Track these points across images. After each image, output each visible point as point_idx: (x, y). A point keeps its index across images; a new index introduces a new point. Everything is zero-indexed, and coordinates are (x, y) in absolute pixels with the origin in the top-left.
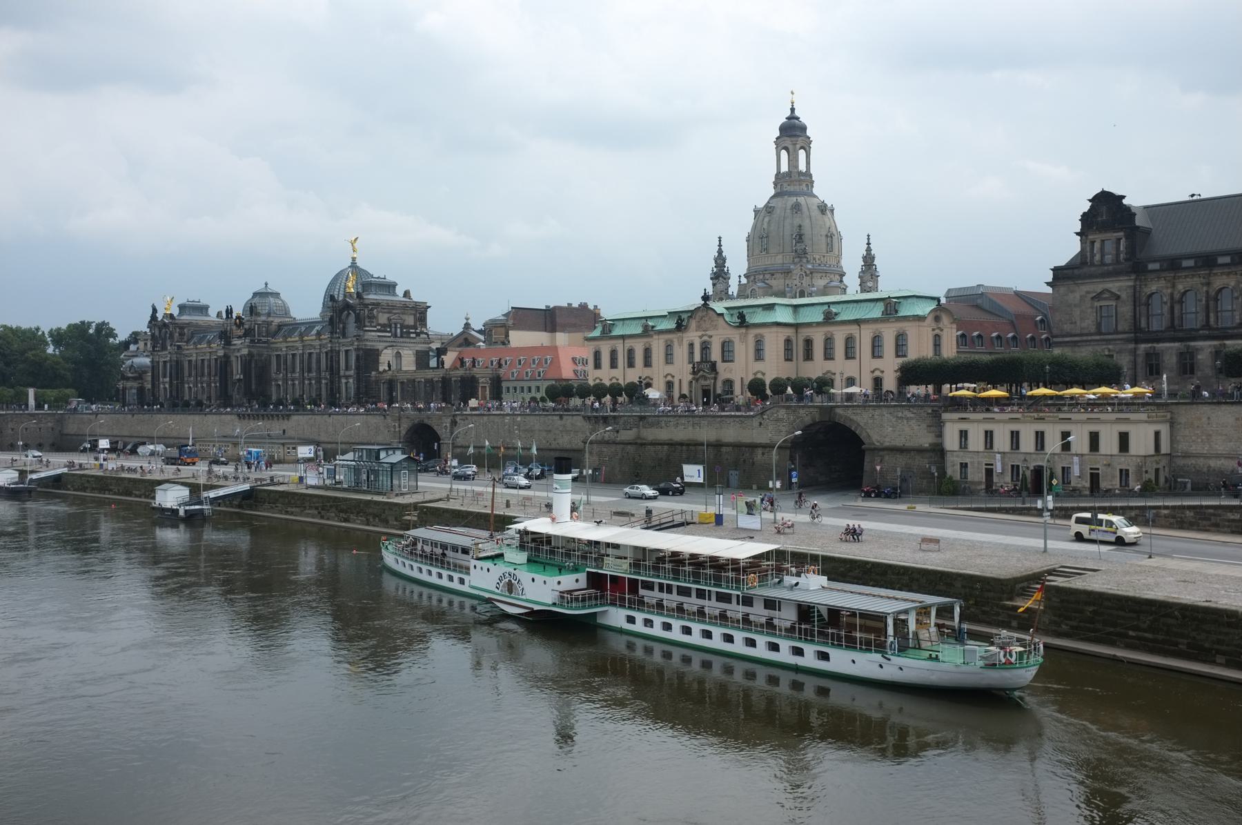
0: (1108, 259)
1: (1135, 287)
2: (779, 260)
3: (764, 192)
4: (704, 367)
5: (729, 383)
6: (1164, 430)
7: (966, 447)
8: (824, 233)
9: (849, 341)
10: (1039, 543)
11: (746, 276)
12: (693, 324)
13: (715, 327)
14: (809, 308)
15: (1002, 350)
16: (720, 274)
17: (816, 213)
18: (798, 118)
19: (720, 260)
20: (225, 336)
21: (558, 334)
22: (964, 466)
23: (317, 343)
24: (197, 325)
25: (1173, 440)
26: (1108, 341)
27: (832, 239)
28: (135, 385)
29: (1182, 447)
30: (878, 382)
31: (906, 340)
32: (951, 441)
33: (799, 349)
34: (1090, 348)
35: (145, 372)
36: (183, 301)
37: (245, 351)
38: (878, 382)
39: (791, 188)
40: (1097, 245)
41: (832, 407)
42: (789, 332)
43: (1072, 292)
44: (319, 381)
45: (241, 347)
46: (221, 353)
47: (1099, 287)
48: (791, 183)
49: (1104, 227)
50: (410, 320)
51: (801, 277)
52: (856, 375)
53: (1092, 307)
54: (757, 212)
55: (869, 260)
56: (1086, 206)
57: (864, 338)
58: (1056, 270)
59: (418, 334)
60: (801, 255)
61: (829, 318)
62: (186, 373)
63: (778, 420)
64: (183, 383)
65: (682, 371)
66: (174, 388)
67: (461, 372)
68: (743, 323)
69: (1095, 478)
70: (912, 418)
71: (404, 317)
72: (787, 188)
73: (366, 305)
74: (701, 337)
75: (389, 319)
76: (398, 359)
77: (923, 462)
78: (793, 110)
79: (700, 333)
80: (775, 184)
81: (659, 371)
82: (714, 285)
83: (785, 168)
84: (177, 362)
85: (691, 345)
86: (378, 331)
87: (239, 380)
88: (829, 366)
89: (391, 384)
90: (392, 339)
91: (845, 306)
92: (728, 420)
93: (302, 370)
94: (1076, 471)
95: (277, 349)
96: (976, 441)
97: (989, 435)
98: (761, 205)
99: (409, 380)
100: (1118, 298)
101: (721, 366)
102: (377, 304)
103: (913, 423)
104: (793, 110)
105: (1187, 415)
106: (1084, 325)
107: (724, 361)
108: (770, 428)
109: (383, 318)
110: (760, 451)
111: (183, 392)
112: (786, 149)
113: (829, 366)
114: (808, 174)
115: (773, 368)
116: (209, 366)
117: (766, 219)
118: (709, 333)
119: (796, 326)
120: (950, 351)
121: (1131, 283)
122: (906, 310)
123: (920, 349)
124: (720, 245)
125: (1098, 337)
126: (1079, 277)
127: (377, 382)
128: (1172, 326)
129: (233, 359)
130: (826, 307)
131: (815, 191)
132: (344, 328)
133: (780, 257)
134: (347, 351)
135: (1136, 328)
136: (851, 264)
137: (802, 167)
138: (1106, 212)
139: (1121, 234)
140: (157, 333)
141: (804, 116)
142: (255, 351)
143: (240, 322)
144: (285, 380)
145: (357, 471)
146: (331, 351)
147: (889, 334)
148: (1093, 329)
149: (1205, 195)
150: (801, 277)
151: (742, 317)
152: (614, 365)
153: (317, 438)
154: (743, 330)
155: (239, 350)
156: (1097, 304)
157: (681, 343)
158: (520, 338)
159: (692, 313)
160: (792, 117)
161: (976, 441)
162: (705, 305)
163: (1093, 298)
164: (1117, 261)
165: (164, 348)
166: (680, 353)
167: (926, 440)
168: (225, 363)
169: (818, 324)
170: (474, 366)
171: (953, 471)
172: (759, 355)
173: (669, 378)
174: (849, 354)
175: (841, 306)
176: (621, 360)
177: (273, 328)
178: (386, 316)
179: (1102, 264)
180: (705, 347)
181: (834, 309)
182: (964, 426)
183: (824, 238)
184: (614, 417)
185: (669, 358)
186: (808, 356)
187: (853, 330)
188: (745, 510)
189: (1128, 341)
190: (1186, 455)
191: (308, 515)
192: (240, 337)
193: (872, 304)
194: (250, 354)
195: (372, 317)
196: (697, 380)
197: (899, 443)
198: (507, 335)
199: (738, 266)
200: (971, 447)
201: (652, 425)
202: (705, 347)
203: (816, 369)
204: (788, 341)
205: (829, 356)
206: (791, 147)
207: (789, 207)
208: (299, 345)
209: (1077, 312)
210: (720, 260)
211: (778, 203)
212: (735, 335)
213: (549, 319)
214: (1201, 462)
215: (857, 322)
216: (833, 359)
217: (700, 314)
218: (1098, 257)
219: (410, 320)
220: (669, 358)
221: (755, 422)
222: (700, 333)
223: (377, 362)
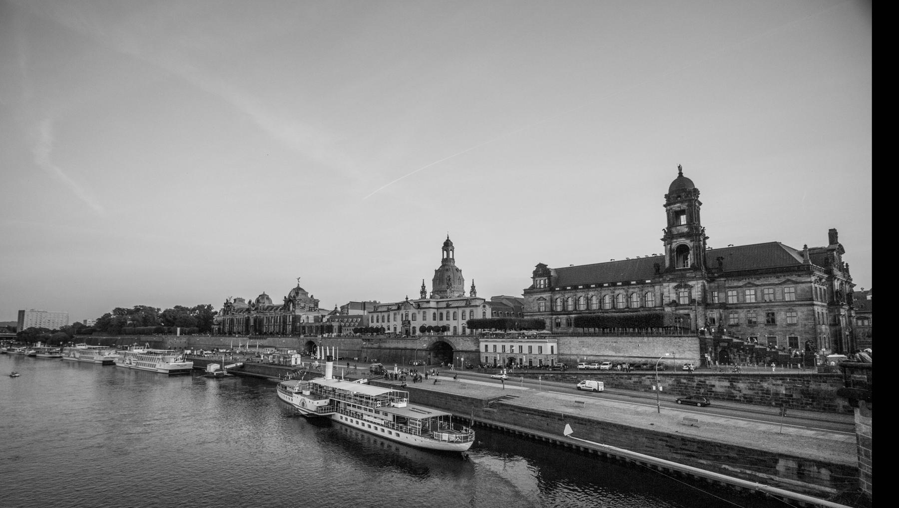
4: (406, 323)
6: (555, 345)
9: (454, 313)
10: (501, 386)
15: (506, 318)
16: (423, 292)
19: (423, 287)
25: (558, 349)
27: (461, 280)
29: (561, 352)
32: (482, 349)
33: (438, 316)
42: (435, 311)
47: (539, 296)
49: (541, 276)
55: (473, 287)
61: (448, 306)
69: (531, 362)
81: (392, 324)
83: (445, 257)
88: (448, 322)
94: (524, 360)
96: (491, 349)
101: (412, 322)
105: (563, 340)
113: (448, 322)
115: (430, 322)
119: (438, 308)
120: (489, 316)
123: (478, 315)
128: (564, 310)
135: (552, 310)
137: (451, 257)
138: (541, 271)
149: (575, 265)
152: (378, 321)
159: (403, 303)
160: (448, 240)
161: (491, 349)
164: (545, 287)
167: (474, 348)
171: (483, 360)
172: (424, 319)
186: (441, 319)
187: (456, 310)
190: (562, 355)
197: (465, 349)
199: (429, 289)
202: (407, 315)
204: (434, 314)
210: (423, 287)
212: (416, 311)
214: (568, 357)
215: (457, 307)
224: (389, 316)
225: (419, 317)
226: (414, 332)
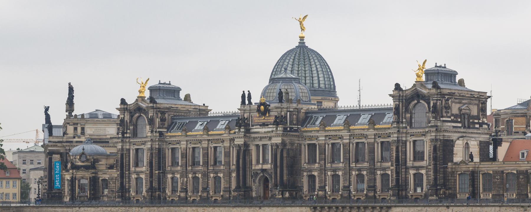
20: (240, 122)
23: (372, 132)
24: (177, 110)
28: (88, 174)
35: (96, 161)
36: (153, 83)
37: (277, 140)
44: (372, 171)
45: (269, 135)
46: (240, 141)
50: (474, 111)
59: (481, 125)
62: (169, 161)
64: (164, 173)
66: (155, 178)
71: (471, 107)
73: (443, 95)
75: (460, 110)
84: (159, 150)
86: (452, 121)
87: (263, 171)
89: (473, 175)
90: (462, 130)
93: (347, 160)
95: (311, 138)
102: (451, 94)
109: (455, 109)
111: (165, 183)
116: (206, 155)
127: (453, 173)
129: (253, 148)
132: (411, 118)
134: (414, 142)
140: (127, 118)
142: (287, 140)
143: (264, 109)
144: (323, 170)
146: (398, 141)
155: (261, 138)
165: (135, 134)
168: (244, 152)
177: (302, 115)
178: (458, 106)
192: (264, 125)
194: (284, 143)
195: (448, 108)
208: (345, 134)
219: (474, 111)
223: (451, 153)
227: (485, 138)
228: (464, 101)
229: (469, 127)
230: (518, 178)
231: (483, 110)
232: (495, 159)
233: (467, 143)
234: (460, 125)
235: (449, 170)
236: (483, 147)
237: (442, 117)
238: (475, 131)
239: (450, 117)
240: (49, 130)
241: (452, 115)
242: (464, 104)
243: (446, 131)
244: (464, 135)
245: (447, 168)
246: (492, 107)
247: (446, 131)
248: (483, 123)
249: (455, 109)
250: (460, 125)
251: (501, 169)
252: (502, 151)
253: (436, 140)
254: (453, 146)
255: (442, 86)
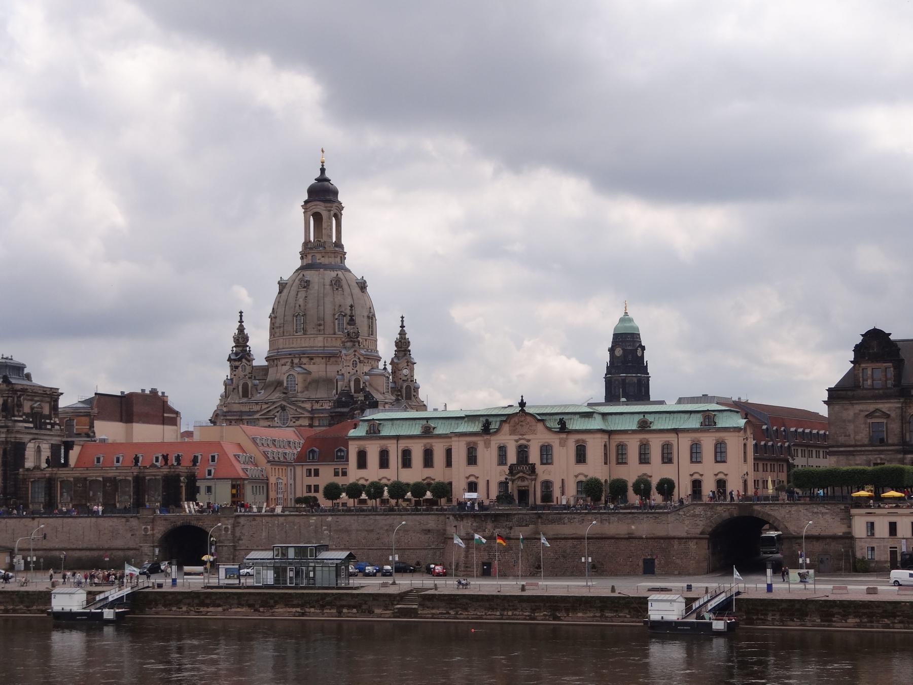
0: (878, 384)
1: (902, 408)
2: (319, 342)
3: (289, 262)
5: (547, 485)
7: (873, 534)
8: (366, 314)
11: (267, 359)
12: (506, 428)
13: (534, 432)
14: (618, 416)
17: (356, 291)
18: (329, 181)
19: (241, 339)
21: (135, 425)
22: (873, 549)
26: (881, 452)
30: (697, 485)
31: (726, 448)
34: (864, 457)
38: (697, 485)
39: (325, 261)
40: (869, 372)
41: (750, 505)
43: (846, 409)
47: (872, 407)
48: (325, 254)
49: (875, 358)
50: (46, 410)
51: (355, 364)
52: (672, 476)
53: (865, 423)
54: (282, 285)
55: (402, 345)
56: (859, 340)
57: (683, 445)
58: (830, 390)
59: (53, 425)
60: (353, 338)
61: (644, 427)
63: (694, 516)
65: (491, 472)
67: (165, 470)
68: (563, 428)
70: (826, 513)
71: (43, 404)
72: (319, 259)
73: (15, 391)
74: (517, 441)
75: (32, 408)
76: (36, 454)
77: (835, 547)
78: (323, 170)
79: (516, 437)
80: (303, 255)
82: (234, 368)
85: (502, 450)
88: (645, 469)
89: (50, 483)
90: (34, 431)
91: (657, 416)
92: (641, 517)
97: (893, 527)
98: (287, 275)
99: (77, 480)
100: (888, 416)
101: (540, 468)
102: (24, 390)
103: (828, 517)
104: (323, 170)
106: (858, 437)
107: (542, 464)
108: (687, 522)
109: (27, 408)
110: (676, 542)
112: (318, 217)
113: (645, 469)
114: (339, 245)
117: (302, 294)
118: (527, 437)
119: (610, 433)
121: (899, 405)
122: (723, 422)
124: (241, 321)
125: (870, 448)
126: (853, 398)
130: (641, 416)
131: (348, 263)
133: (320, 338)
135: (903, 442)
136: (386, 349)
139: (890, 364)
141: (335, 180)
145: (280, 572)
147: (708, 443)
148: (866, 441)
150: (355, 364)
151: (562, 423)
152: (384, 462)
153: (9, 545)
154: (564, 436)
156: (869, 421)
157: (487, 445)
158: (108, 430)
160: (323, 179)
161: (882, 529)
162: (522, 410)
163: (867, 416)
166: (487, 455)
169: (634, 432)
170: (179, 464)
172: (581, 456)
173: (472, 479)
174: (667, 458)
175: (653, 416)
176: (394, 459)
179: (873, 388)
180: (523, 452)
181: (650, 418)
182: (871, 519)
183: (366, 319)
184: (508, 515)
185: (472, 459)
187: (672, 438)
188: (798, 579)
189: (898, 452)
191: (236, 613)
193: (686, 416)
195: (20, 405)
196: (513, 481)
198: (92, 426)
200: (877, 535)
201: (552, 522)
202: (523, 452)
203: (631, 472)
205: (644, 458)
206: (325, 214)
207: (327, 282)
209: (851, 428)
210: (241, 339)
211: (309, 275)
212: (554, 440)
213: (125, 408)
215: (676, 431)
216: (649, 463)
217: (516, 419)
218: (869, 382)
219: (46, 410)
220: (472, 459)
221: (671, 518)
222: (516, 437)
224: (449, 452)
225: (564, 454)
226: (547, 496)
227: (56, 440)
228: (36, 399)
229: (41, 428)
230: (105, 485)
231: (55, 407)
232: (66, 464)
233: (39, 447)
234: (31, 425)
235: (21, 477)
236: (55, 449)
237: (14, 416)
238: (48, 432)
239: (21, 416)
240: (527, 458)
241: (24, 414)
242: (37, 401)
243: (18, 432)
244: (36, 436)
245: (18, 474)
246: (63, 403)
247: (18, 432)
248: (55, 424)
249: (27, 408)
250: (31, 425)
251: (84, 476)
252: (74, 454)
253: (7, 442)
254: (25, 450)
255: (13, 381)
